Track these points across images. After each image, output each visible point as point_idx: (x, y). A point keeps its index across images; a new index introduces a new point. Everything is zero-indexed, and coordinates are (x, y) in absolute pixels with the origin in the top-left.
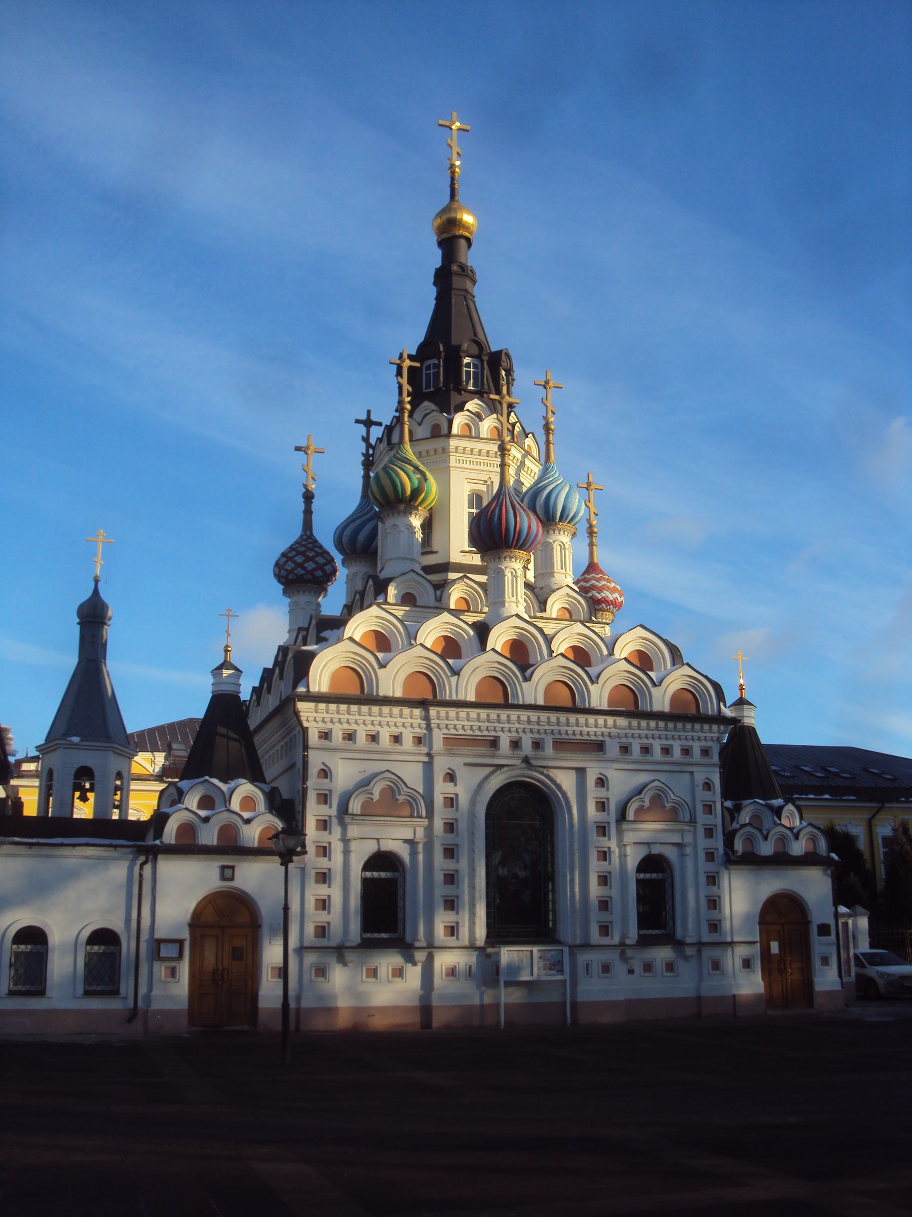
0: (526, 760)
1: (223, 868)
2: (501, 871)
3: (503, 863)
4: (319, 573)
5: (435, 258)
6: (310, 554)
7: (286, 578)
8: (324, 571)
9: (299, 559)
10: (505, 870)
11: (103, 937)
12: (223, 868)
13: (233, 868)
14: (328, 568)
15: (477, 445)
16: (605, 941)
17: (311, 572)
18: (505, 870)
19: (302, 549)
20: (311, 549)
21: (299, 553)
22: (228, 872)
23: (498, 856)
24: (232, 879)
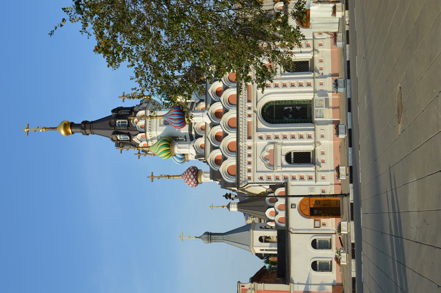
0: (255, 111)
1: (292, 208)
2: (290, 117)
3: (288, 117)
4: (194, 174)
5: (79, 135)
6: (188, 177)
7: (196, 184)
8: (193, 172)
9: (190, 180)
10: (290, 115)
11: (314, 244)
12: (292, 208)
13: (292, 205)
14: (193, 170)
15: (148, 123)
16: (312, 84)
17: (194, 176)
18: (290, 115)
19: (187, 179)
20: (186, 176)
21: (188, 180)
22: (293, 206)
23: (286, 119)
24: (295, 205)
